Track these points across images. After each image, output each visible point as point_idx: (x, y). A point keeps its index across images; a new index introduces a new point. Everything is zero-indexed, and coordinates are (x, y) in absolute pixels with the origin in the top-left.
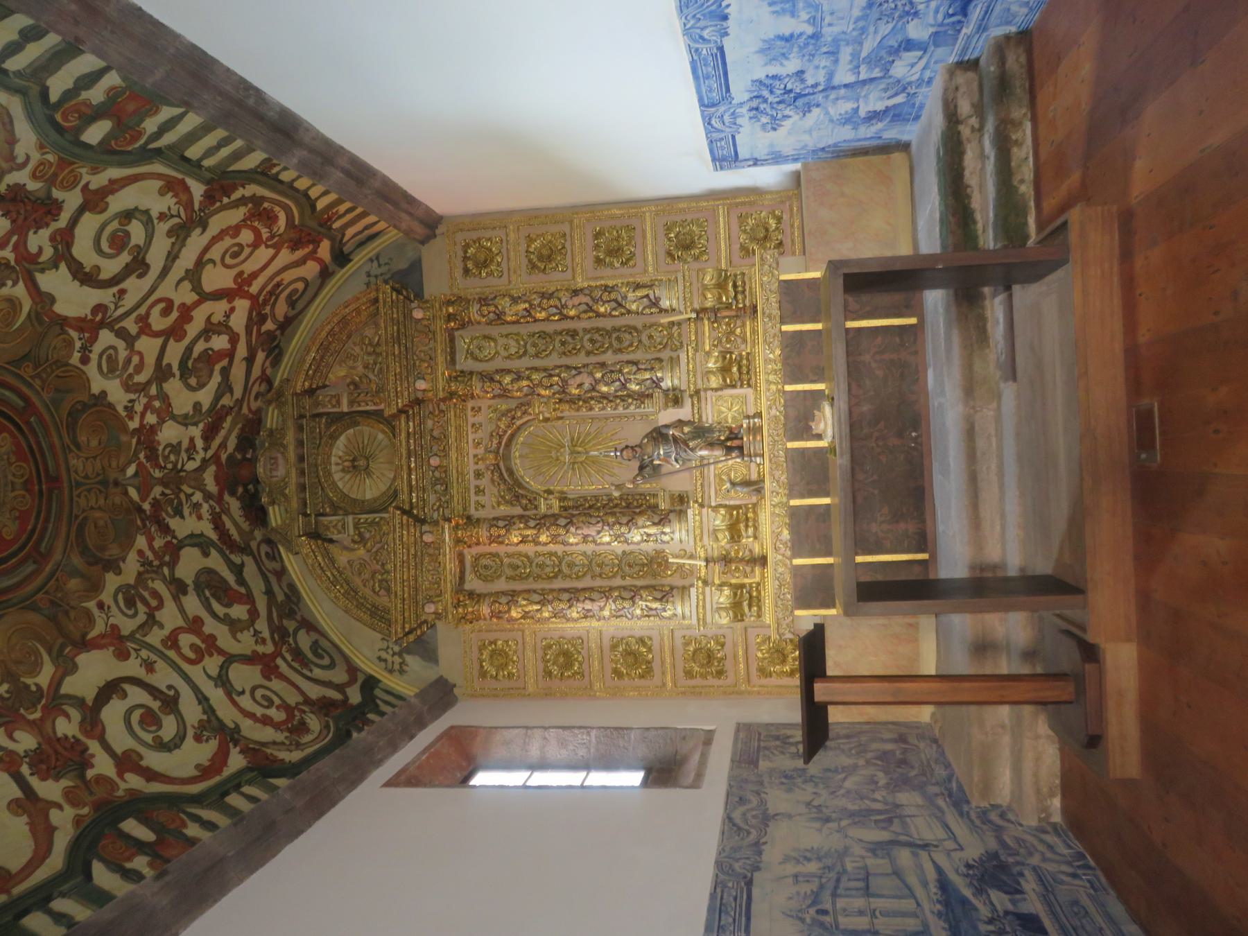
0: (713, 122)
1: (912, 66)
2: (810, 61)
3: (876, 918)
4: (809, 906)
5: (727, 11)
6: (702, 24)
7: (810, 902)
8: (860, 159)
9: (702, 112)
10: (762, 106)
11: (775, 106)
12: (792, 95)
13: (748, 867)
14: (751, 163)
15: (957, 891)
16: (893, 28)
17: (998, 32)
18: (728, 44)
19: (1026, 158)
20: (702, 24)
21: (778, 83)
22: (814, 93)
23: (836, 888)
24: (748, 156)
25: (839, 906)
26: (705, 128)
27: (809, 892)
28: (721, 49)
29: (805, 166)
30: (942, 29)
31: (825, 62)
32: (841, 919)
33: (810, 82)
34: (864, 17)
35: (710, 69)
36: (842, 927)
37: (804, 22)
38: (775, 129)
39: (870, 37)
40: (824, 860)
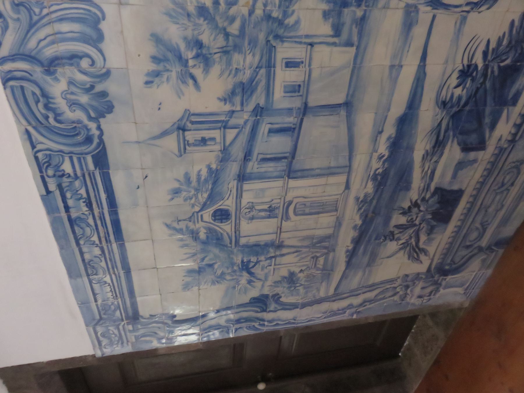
3: (288, 218)
4: (204, 207)
7: (206, 195)
13: (84, 99)
15: (411, 149)
23: (247, 156)
25: (247, 198)
27: (204, 173)
32: (246, 227)
36: (243, 241)
40: (237, 58)
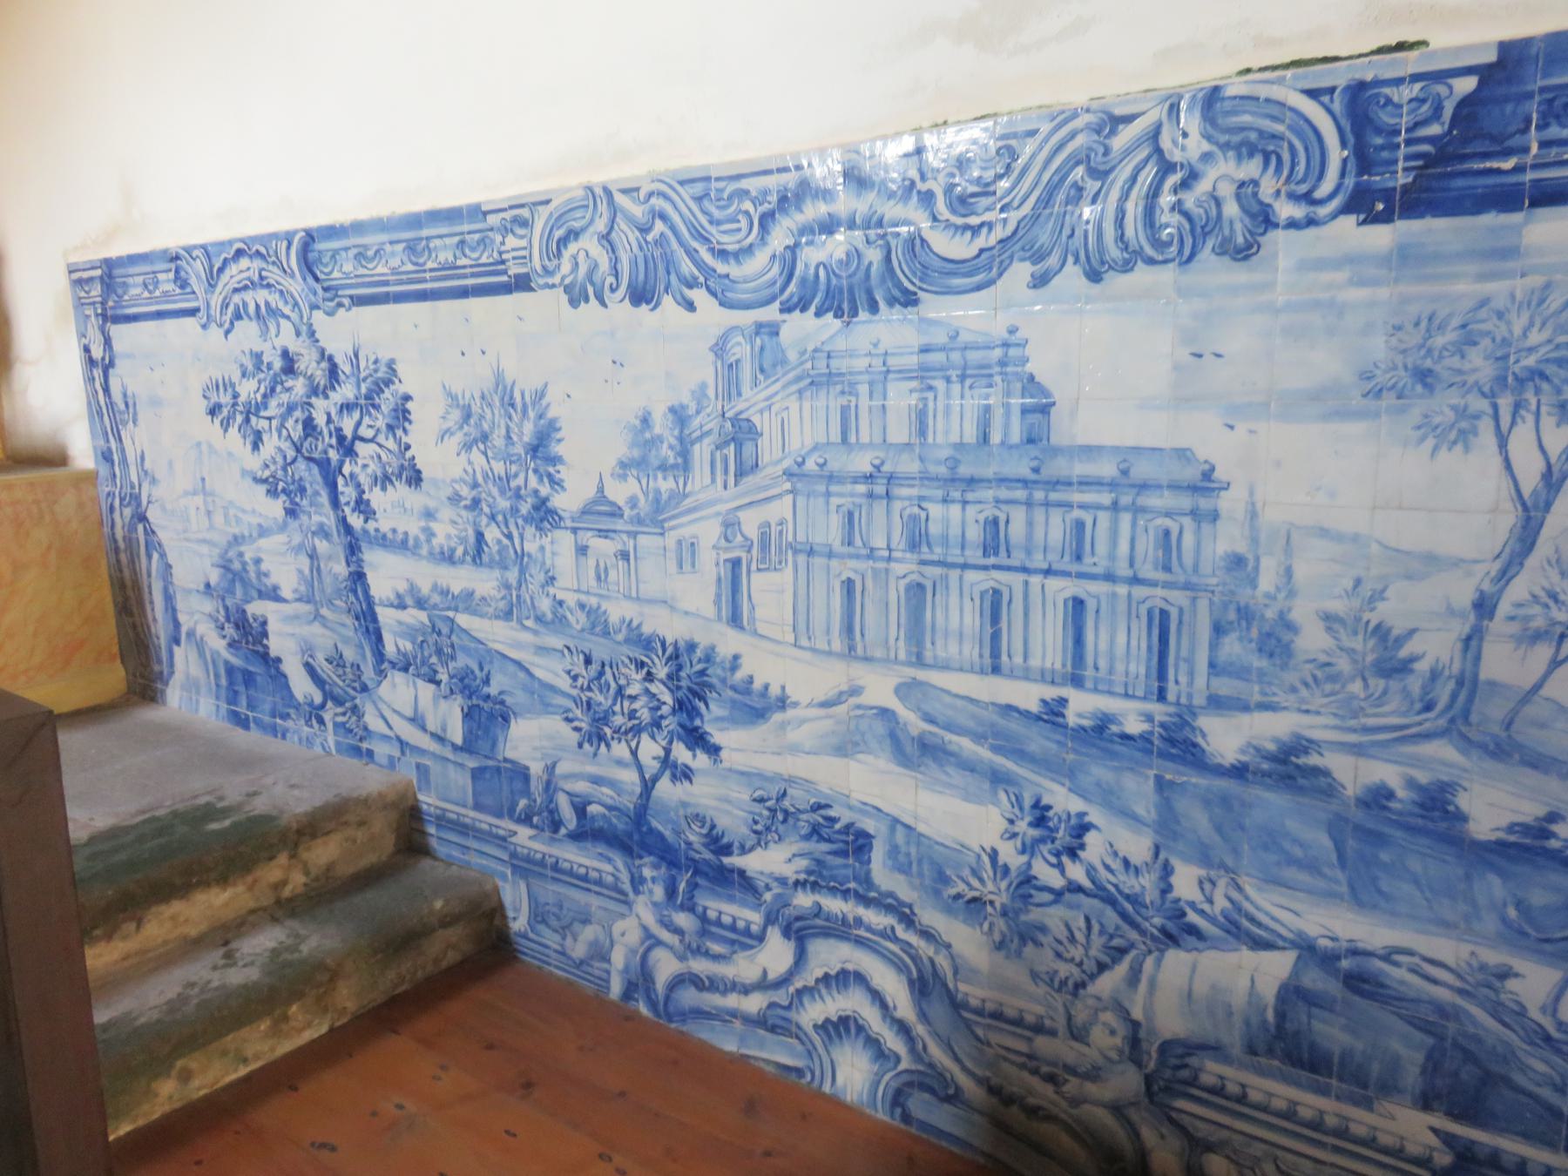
0: (244, 262)
1: (417, 720)
2: (455, 499)
5: (668, 301)
6: (626, 237)
8: (105, 597)
9: (288, 237)
10: (299, 386)
11: (298, 414)
12: (333, 455)
14: (97, 352)
16: (552, 688)
17: (516, 900)
18: (543, 305)
19: (245, 1061)
20: (626, 237)
21: (381, 423)
22: (335, 503)
24: (117, 346)
26: (222, 245)
28: (522, 284)
29: (90, 478)
30: (536, 787)
31: (448, 529)
33: (376, 497)
34: (598, 623)
35: (445, 256)
37: (601, 490)
38: (213, 411)
39: (527, 637)
